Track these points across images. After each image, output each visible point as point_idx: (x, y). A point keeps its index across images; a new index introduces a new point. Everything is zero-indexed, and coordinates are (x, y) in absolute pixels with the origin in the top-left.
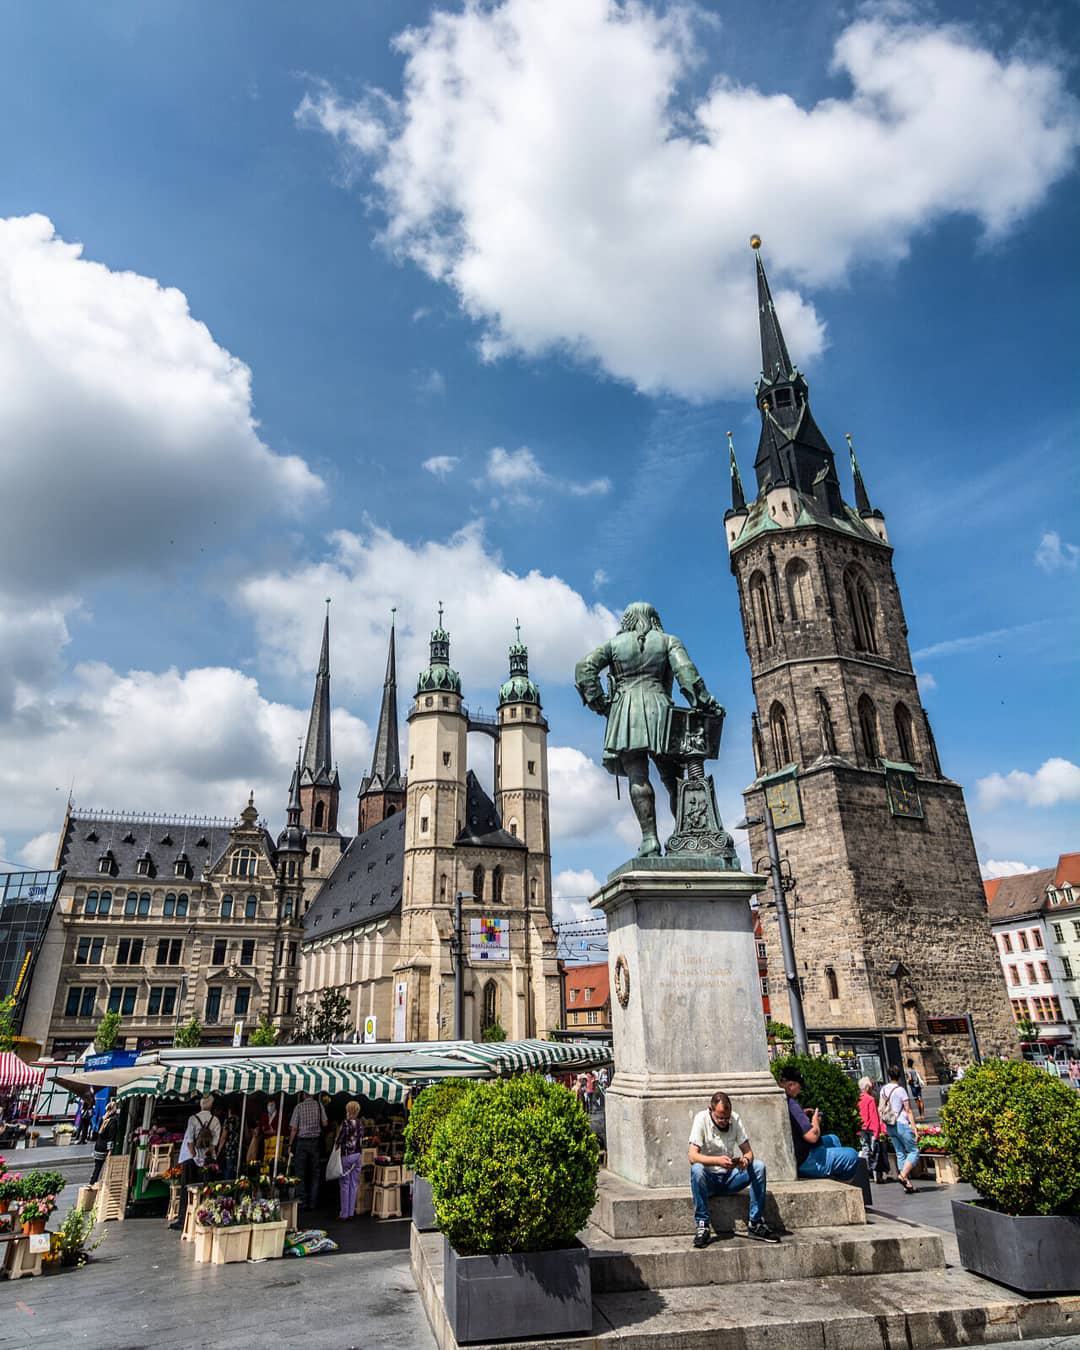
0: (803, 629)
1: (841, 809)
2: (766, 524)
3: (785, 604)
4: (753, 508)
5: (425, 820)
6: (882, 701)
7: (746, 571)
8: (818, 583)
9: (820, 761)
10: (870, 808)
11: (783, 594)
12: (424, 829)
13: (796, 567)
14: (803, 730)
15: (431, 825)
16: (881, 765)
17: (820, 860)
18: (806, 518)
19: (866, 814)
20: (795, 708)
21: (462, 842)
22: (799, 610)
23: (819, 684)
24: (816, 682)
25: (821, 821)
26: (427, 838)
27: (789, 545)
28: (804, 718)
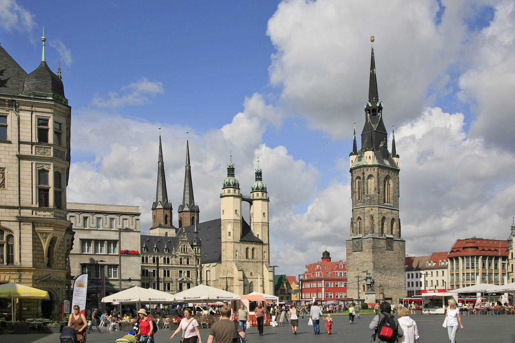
0: (370, 197)
1: (373, 248)
2: (363, 162)
3: (366, 189)
4: (360, 153)
5: (230, 233)
6: (388, 218)
7: (355, 176)
8: (376, 184)
9: (369, 235)
10: (380, 248)
11: (365, 186)
12: (230, 235)
13: (370, 176)
14: (366, 226)
15: (231, 235)
16: (385, 236)
17: (366, 260)
18: (376, 162)
19: (379, 249)
20: (364, 220)
21: (242, 241)
22: (369, 190)
23: (372, 214)
24: (371, 213)
25: (367, 251)
26: (231, 238)
27: (369, 170)
28: (367, 223)
